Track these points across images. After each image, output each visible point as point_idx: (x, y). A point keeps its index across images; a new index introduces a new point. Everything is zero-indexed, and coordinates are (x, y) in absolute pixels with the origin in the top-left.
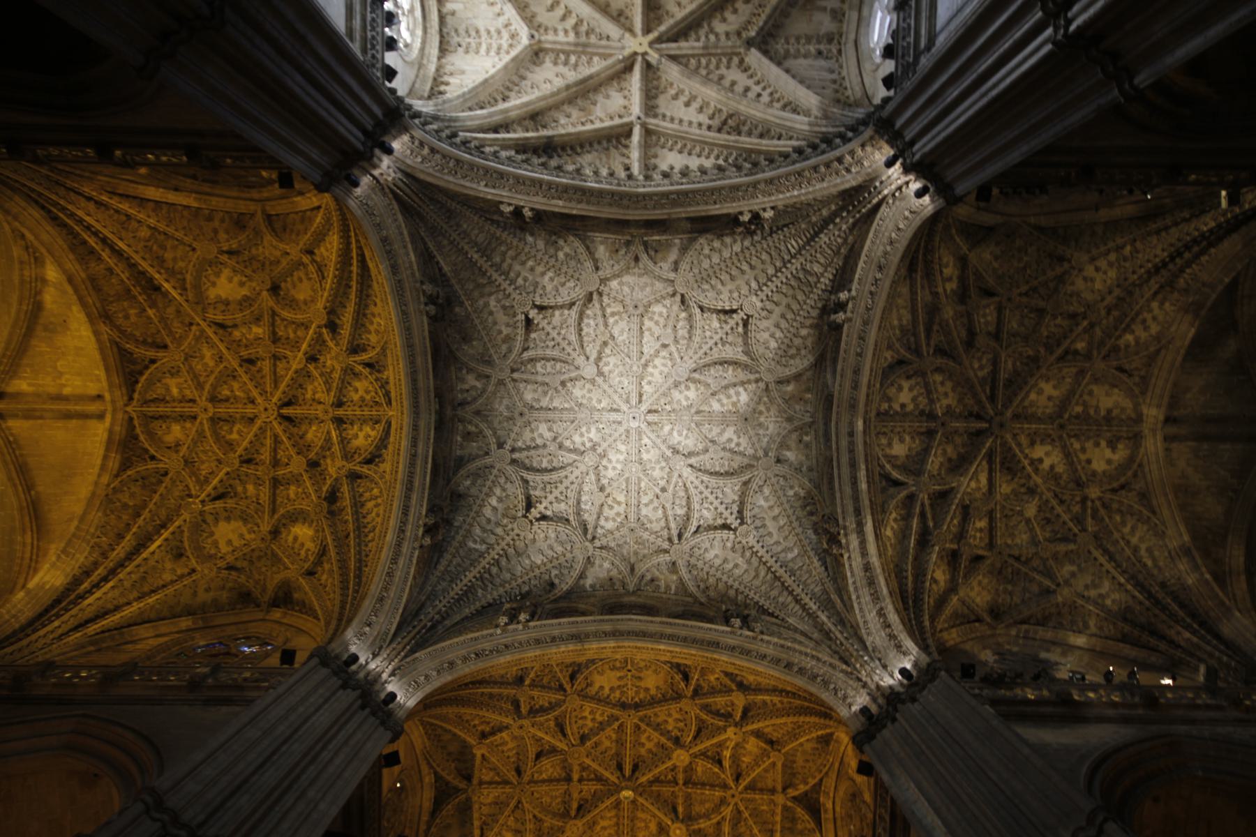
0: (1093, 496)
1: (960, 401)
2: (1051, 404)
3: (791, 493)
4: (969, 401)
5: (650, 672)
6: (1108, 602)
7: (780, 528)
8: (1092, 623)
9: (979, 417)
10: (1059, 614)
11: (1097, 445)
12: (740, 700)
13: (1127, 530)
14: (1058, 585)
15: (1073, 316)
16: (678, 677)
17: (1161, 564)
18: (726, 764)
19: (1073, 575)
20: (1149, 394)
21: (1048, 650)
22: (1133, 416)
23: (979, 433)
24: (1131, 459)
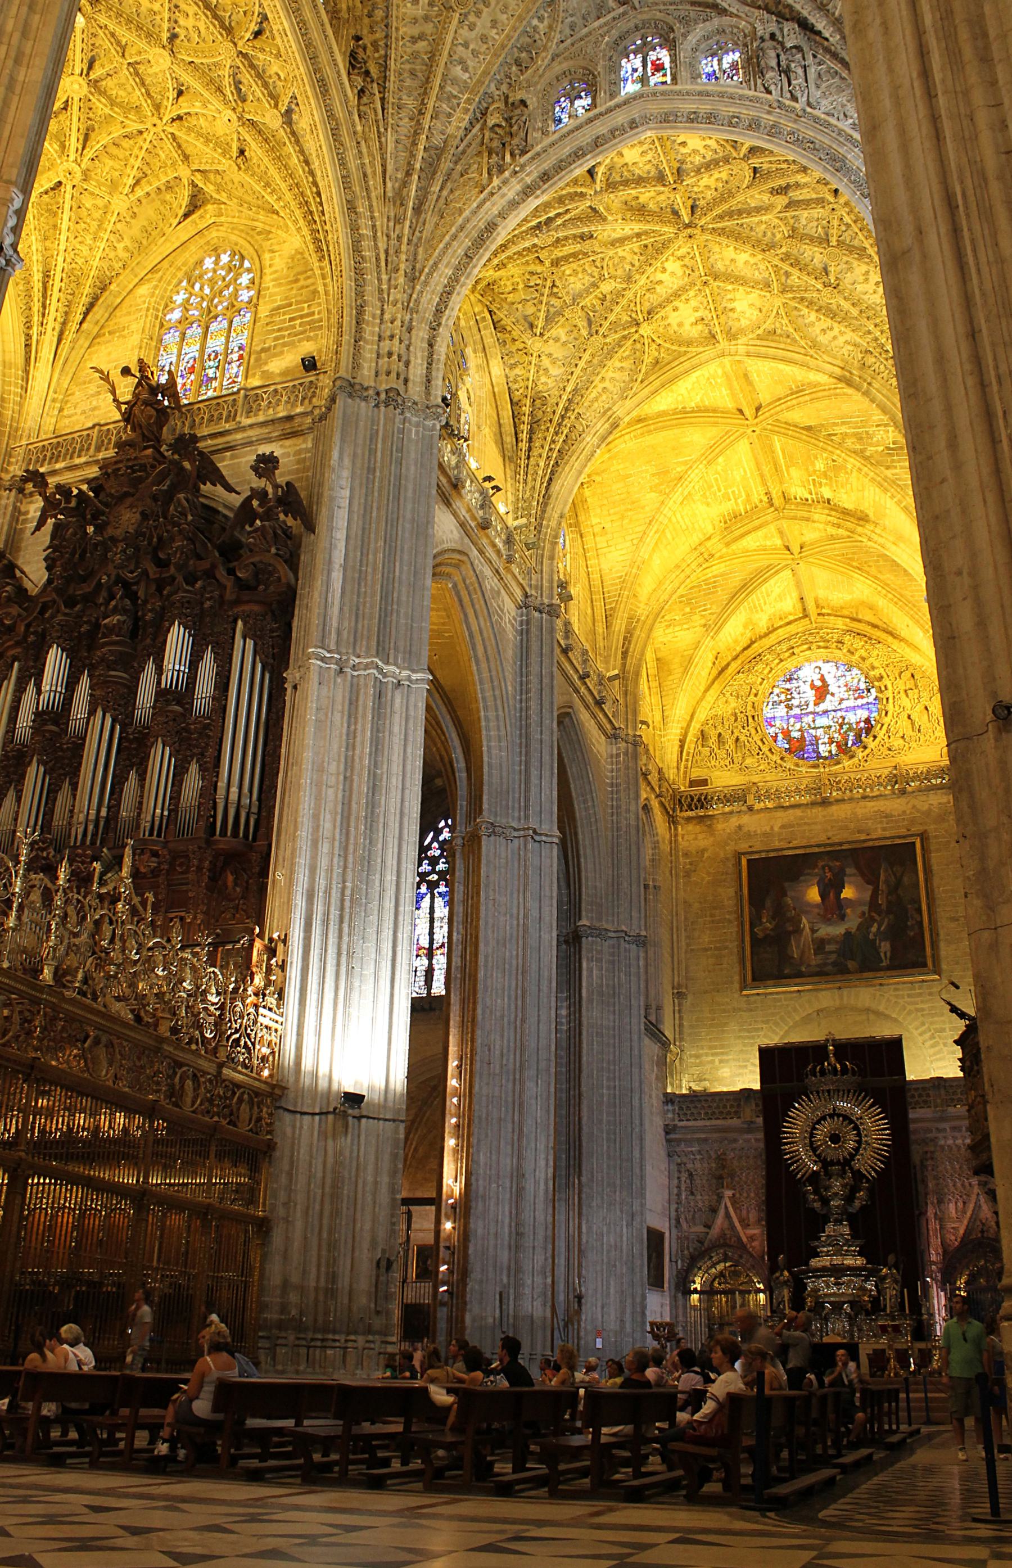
0: (641, 331)
1: (708, 187)
4: (709, 195)
6: (543, 379)
7: (484, 39)
8: (518, 371)
9: (693, 208)
11: (696, 310)
12: (272, 120)
13: (618, 365)
14: (541, 334)
15: (826, 270)
17: (596, 405)
18: (184, 106)
19: (557, 340)
20: (758, 342)
21: (475, 351)
22: (733, 330)
23: (676, 213)
24: (689, 343)
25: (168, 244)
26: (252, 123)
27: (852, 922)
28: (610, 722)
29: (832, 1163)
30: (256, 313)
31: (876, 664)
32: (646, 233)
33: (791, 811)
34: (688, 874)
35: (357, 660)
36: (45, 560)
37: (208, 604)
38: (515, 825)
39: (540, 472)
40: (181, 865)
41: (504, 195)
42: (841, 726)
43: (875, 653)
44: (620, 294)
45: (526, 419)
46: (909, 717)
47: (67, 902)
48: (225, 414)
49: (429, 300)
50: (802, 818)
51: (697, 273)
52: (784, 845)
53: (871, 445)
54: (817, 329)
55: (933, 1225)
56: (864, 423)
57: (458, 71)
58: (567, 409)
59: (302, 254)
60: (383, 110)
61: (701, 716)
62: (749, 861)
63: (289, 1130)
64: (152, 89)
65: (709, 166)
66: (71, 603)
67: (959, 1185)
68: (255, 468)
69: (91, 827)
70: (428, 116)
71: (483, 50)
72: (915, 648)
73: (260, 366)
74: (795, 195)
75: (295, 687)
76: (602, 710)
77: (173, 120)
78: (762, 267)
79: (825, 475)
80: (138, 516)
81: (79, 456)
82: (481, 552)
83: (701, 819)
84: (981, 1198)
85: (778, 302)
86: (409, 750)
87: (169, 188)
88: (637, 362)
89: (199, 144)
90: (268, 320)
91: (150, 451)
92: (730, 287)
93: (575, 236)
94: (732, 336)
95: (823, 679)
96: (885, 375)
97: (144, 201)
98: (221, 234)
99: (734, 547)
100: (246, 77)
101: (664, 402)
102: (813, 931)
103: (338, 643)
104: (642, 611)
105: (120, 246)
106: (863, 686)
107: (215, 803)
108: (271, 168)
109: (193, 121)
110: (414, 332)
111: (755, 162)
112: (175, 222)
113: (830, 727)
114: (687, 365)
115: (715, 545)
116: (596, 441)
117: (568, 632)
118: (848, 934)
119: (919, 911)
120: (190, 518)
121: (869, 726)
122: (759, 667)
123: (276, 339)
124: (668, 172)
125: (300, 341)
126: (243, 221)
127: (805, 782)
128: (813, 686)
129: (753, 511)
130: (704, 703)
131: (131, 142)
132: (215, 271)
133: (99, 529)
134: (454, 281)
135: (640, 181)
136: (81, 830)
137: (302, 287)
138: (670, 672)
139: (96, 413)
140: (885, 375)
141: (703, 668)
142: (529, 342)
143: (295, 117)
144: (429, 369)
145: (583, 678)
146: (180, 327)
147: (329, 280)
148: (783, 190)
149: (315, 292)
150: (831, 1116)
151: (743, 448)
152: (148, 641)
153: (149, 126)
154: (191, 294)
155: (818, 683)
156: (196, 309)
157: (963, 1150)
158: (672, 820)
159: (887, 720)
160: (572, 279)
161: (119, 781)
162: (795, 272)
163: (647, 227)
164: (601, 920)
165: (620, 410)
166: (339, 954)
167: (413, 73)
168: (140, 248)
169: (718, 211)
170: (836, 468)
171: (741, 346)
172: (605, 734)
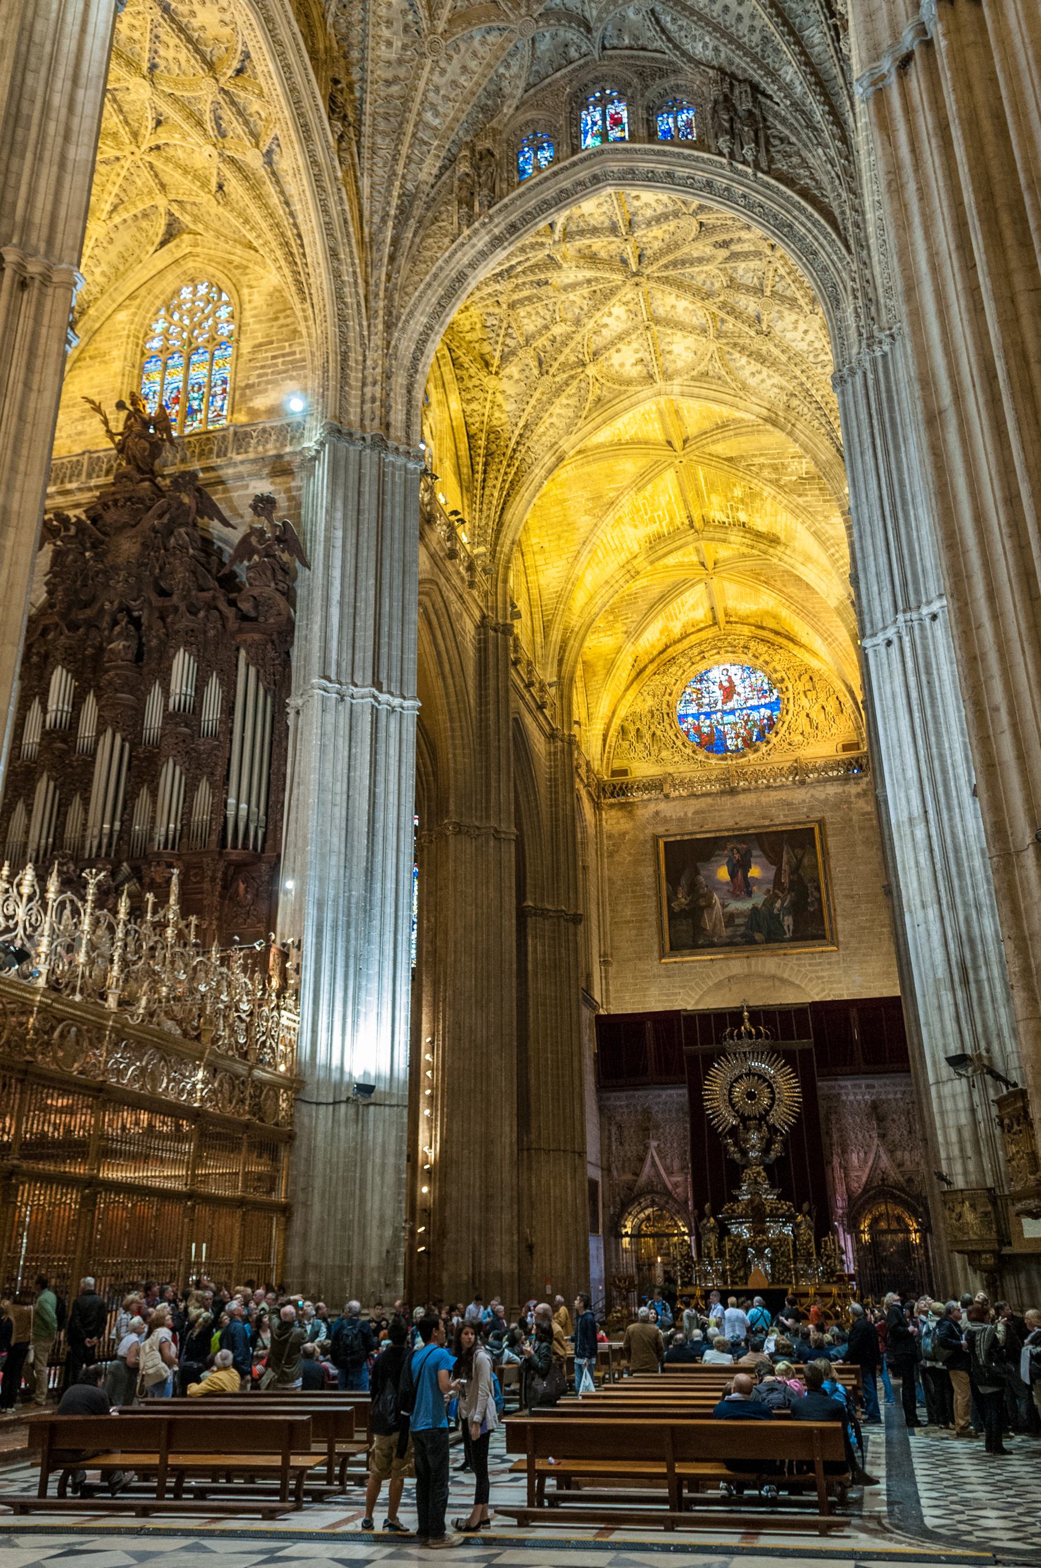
1: (656, 238)
2: (668, 308)
3: (502, 70)
4: (657, 245)
5: (219, 16)
6: (497, 414)
8: (474, 406)
10: (471, 377)
12: (253, 159)
13: (565, 401)
14: (497, 373)
16: (236, 65)
18: (163, 137)
19: (510, 377)
20: (692, 383)
22: (670, 371)
23: (624, 262)
24: (629, 382)
25: (145, 272)
26: (232, 161)
27: (758, 899)
28: (549, 723)
29: (749, 1118)
30: (238, 348)
31: (778, 668)
32: (596, 279)
33: (703, 799)
34: (611, 855)
35: (355, 690)
36: (47, 584)
37: (212, 633)
38: (477, 824)
39: (495, 502)
40: (196, 875)
41: (474, 246)
42: (746, 722)
43: (778, 657)
44: (569, 337)
45: (482, 452)
46: (808, 715)
47: (127, 933)
48: (215, 448)
49: (406, 346)
50: (712, 805)
51: (640, 318)
52: (696, 829)
53: (786, 475)
54: (746, 373)
55: (839, 1173)
56: (780, 456)
57: (428, 116)
58: (518, 443)
59: (280, 291)
60: (359, 153)
61: (622, 713)
62: (666, 843)
63: (306, 1120)
64: (130, 117)
65: (660, 219)
66: (73, 627)
67: (860, 1137)
68: (254, 507)
69: (105, 841)
70: (401, 163)
71: (451, 96)
72: (814, 654)
73: (245, 402)
74: (736, 248)
75: (298, 713)
76: (543, 713)
77: (151, 149)
78: (700, 313)
79: (742, 501)
80: (138, 546)
81: (70, 482)
82: (448, 580)
83: (622, 806)
84: (881, 1150)
85: (713, 347)
86: (403, 770)
87: (145, 215)
88: (583, 400)
89: (177, 175)
90: (251, 356)
91: (147, 484)
92: (669, 332)
93: (532, 282)
94: (668, 376)
95: (730, 680)
96: (808, 417)
97: (121, 227)
98: (197, 265)
99: (656, 564)
100: (227, 114)
101: (604, 436)
102: (724, 906)
103: (338, 674)
104: (575, 621)
105: (98, 271)
106: (766, 687)
107: (225, 817)
108: (250, 204)
109: (171, 152)
110: (393, 379)
111: (703, 217)
112: (152, 249)
113: (736, 724)
114: (626, 403)
115: (641, 563)
116: (543, 472)
117: (517, 647)
118: (755, 909)
119: (818, 889)
120: (191, 551)
121: (771, 724)
122: (674, 669)
123: (260, 376)
124: (621, 224)
125: (283, 380)
126: (220, 254)
127: (715, 773)
128: (721, 686)
129: (675, 533)
130: (624, 701)
131: (108, 168)
132: (193, 302)
133: (99, 557)
134: (429, 328)
135: (595, 231)
136: (95, 843)
137: (282, 326)
138: (594, 674)
139: (82, 437)
140: (808, 417)
141: (624, 671)
142: (486, 380)
143: (275, 158)
144: (408, 413)
145: (529, 685)
146: (162, 357)
147: (311, 322)
148: (725, 244)
149: (295, 331)
150: (747, 1075)
151: (669, 477)
152: (153, 665)
153: (127, 153)
154: (171, 324)
155: (726, 684)
156: (177, 339)
157: (863, 1105)
158: (597, 807)
159: (788, 718)
160: (526, 321)
161: (131, 797)
162: (731, 320)
163: (599, 274)
164: (542, 901)
165: (565, 444)
166: (347, 957)
167: (386, 117)
168: (117, 274)
169: (664, 261)
170: (753, 495)
171: (676, 386)
172: (544, 734)
